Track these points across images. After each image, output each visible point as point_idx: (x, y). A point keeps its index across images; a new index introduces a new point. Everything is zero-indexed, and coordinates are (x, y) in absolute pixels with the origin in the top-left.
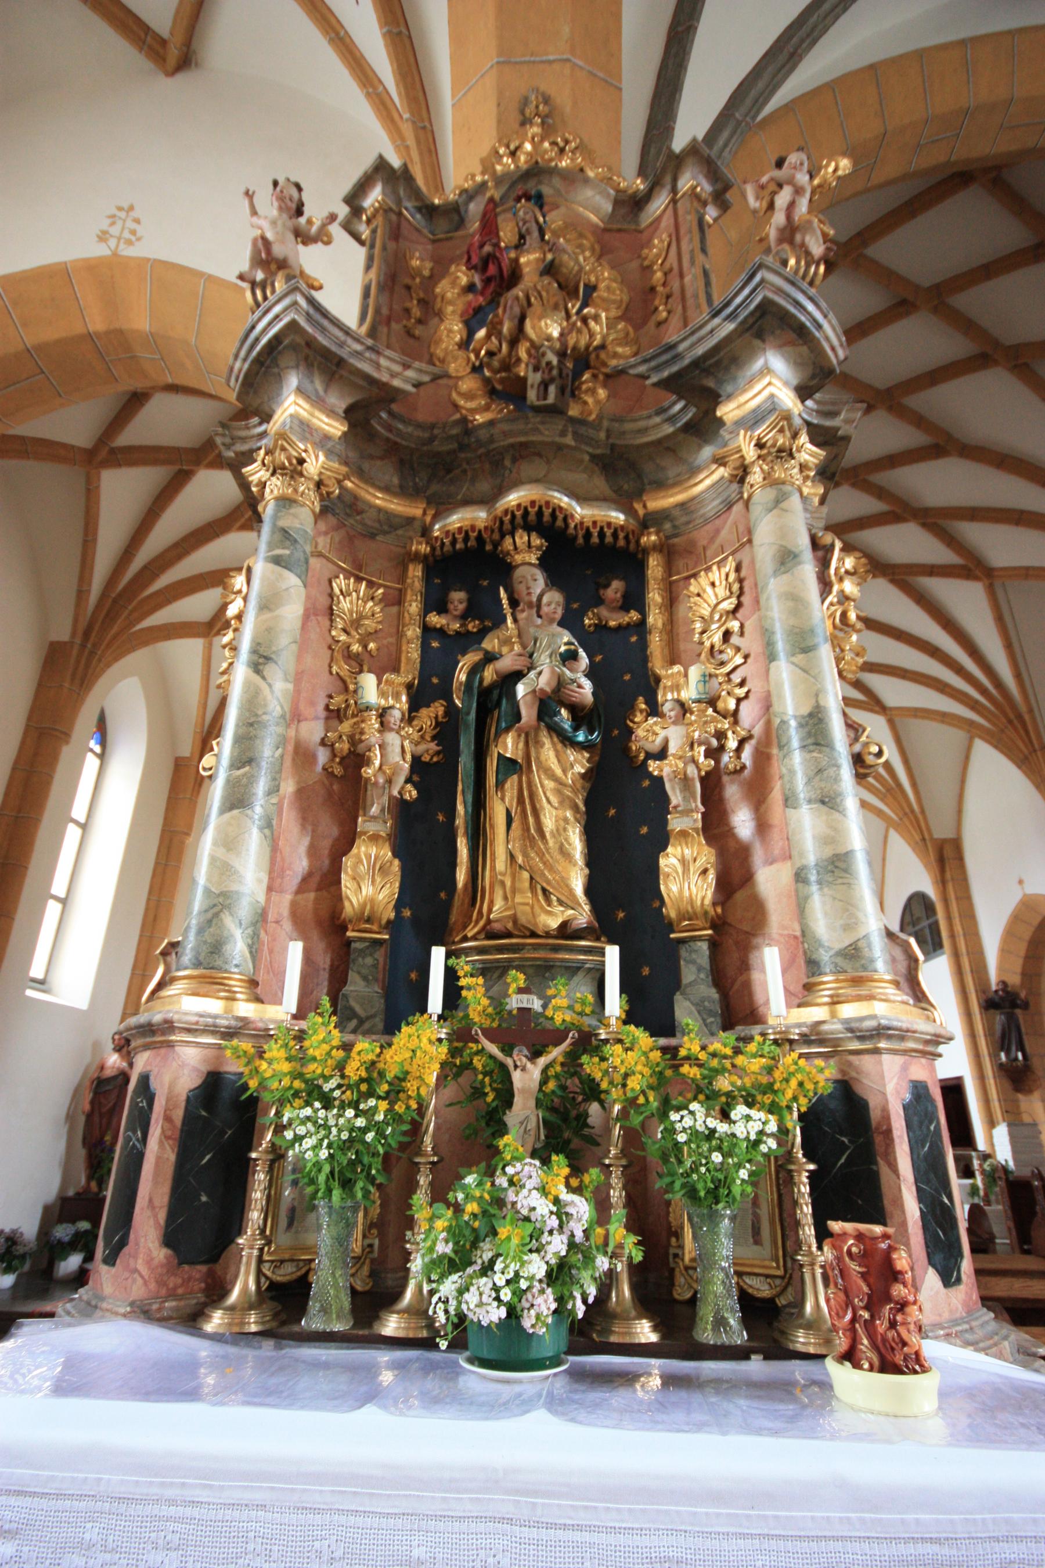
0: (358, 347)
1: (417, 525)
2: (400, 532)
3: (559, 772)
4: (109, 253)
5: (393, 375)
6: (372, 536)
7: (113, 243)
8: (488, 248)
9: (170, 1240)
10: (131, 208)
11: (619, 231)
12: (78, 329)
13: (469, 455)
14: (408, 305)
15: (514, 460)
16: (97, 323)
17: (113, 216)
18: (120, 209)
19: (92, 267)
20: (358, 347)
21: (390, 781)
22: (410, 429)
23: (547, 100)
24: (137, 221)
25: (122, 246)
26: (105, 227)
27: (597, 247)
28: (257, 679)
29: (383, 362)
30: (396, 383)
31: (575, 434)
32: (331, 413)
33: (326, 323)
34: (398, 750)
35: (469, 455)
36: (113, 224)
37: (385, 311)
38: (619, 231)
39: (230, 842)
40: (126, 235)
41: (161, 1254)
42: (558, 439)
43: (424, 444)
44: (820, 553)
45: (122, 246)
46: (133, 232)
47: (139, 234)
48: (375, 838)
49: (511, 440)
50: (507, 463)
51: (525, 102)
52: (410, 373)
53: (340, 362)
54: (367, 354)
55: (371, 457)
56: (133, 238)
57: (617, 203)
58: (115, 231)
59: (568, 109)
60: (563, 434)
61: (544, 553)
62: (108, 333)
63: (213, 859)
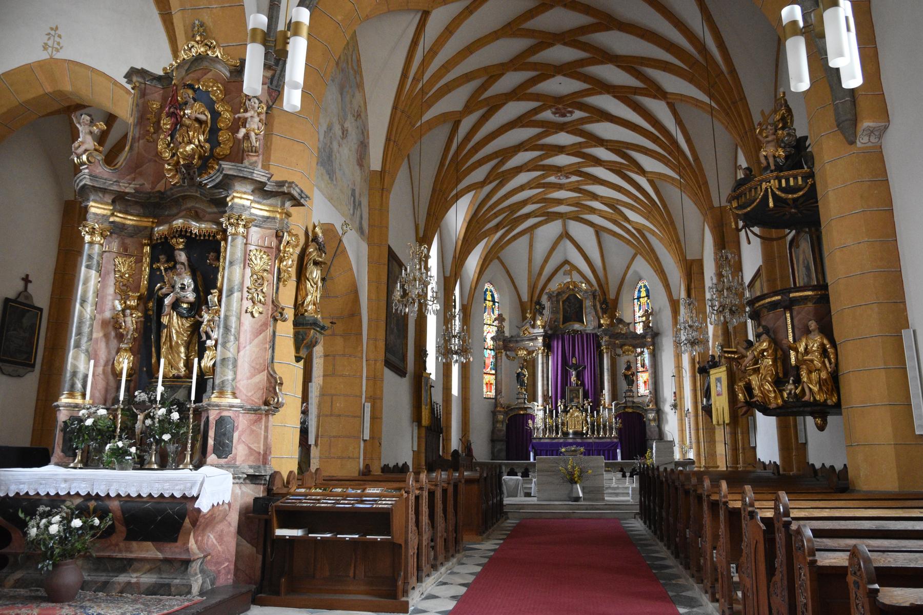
0: (111, 182)
1: (149, 229)
2: (143, 232)
3: (177, 328)
4: (49, 57)
5: (126, 187)
6: (132, 237)
7: (50, 49)
8: (172, 110)
9: (63, 451)
10: (57, 28)
11: (234, 82)
12: (41, 92)
13: (164, 202)
14: (148, 128)
15: (183, 200)
16: (49, 89)
17: (49, 34)
18: (52, 29)
19: (41, 64)
20: (111, 182)
21: (128, 332)
22: (141, 195)
23: (202, 25)
24: (60, 36)
25: (54, 52)
26: (46, 42)
27: (224, 92)
28: (81, 308)
29: (121, 184)
30: (127, 190)
31: (200, 192)
32: (107, 204)
33: (97, 179)
34: (130, 322)
35: (164, 202)
36: (49, 39)
37: (137, 136)
38: (234, 82)
39: (76, 358)
40: (56, 46)
41: (61, 454)
42: (194, 194)
43: (148, 200)
44: (280, 238)
45: (54, 52)
46: (59, 43)
47: (61, 45)
48: (125, 350)
49: (179, 195)
50: (181, 200)
51: (193, 25)
52: (131, 186)
53: (105, 189)
54: (115, 183)
55: (130, 205)
56: (59, 48)
57: (231, 72)
58: (50, 43)
59: (212, 27)
60: (196, 192)
61: (186, 243)
62: (54, 92)
63: (71, 363)
